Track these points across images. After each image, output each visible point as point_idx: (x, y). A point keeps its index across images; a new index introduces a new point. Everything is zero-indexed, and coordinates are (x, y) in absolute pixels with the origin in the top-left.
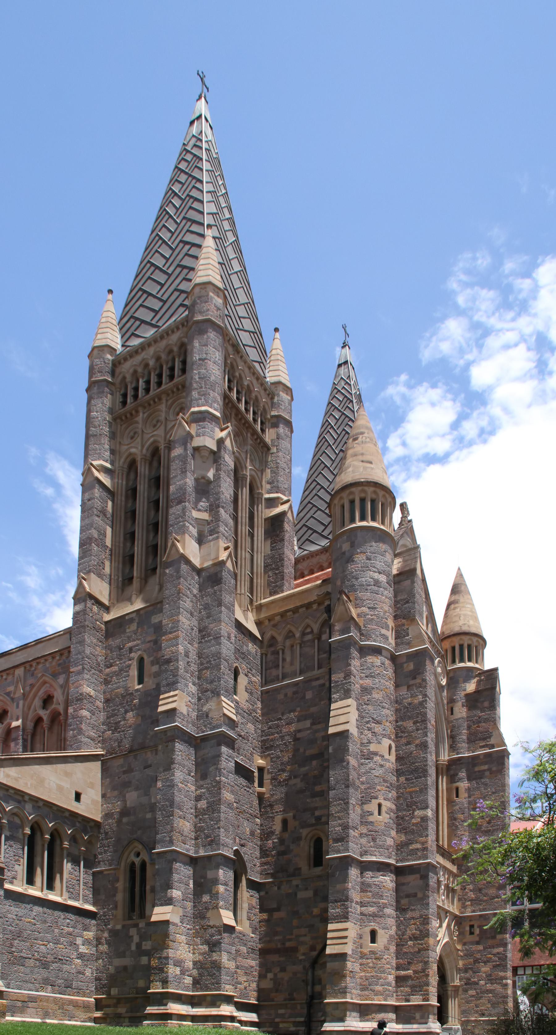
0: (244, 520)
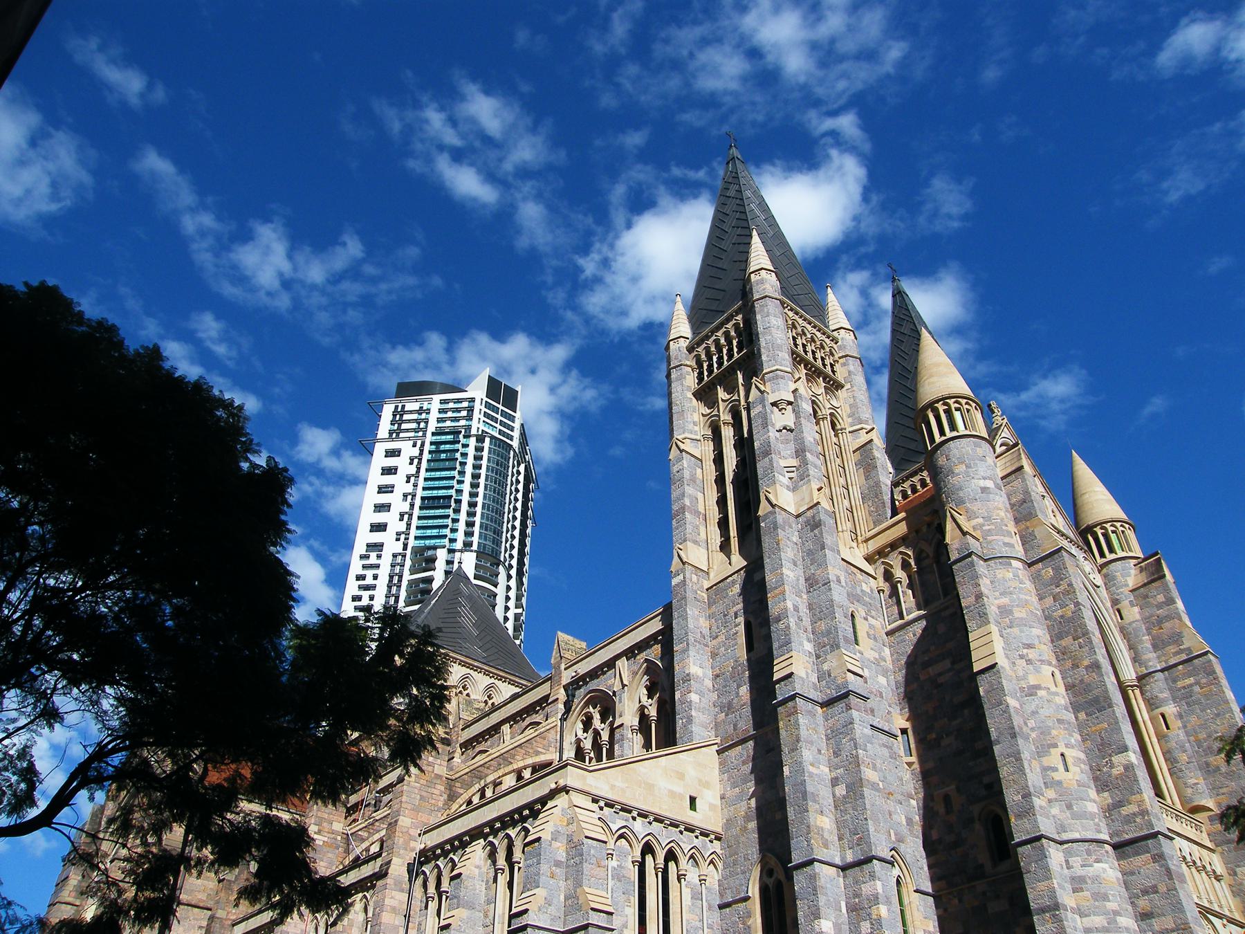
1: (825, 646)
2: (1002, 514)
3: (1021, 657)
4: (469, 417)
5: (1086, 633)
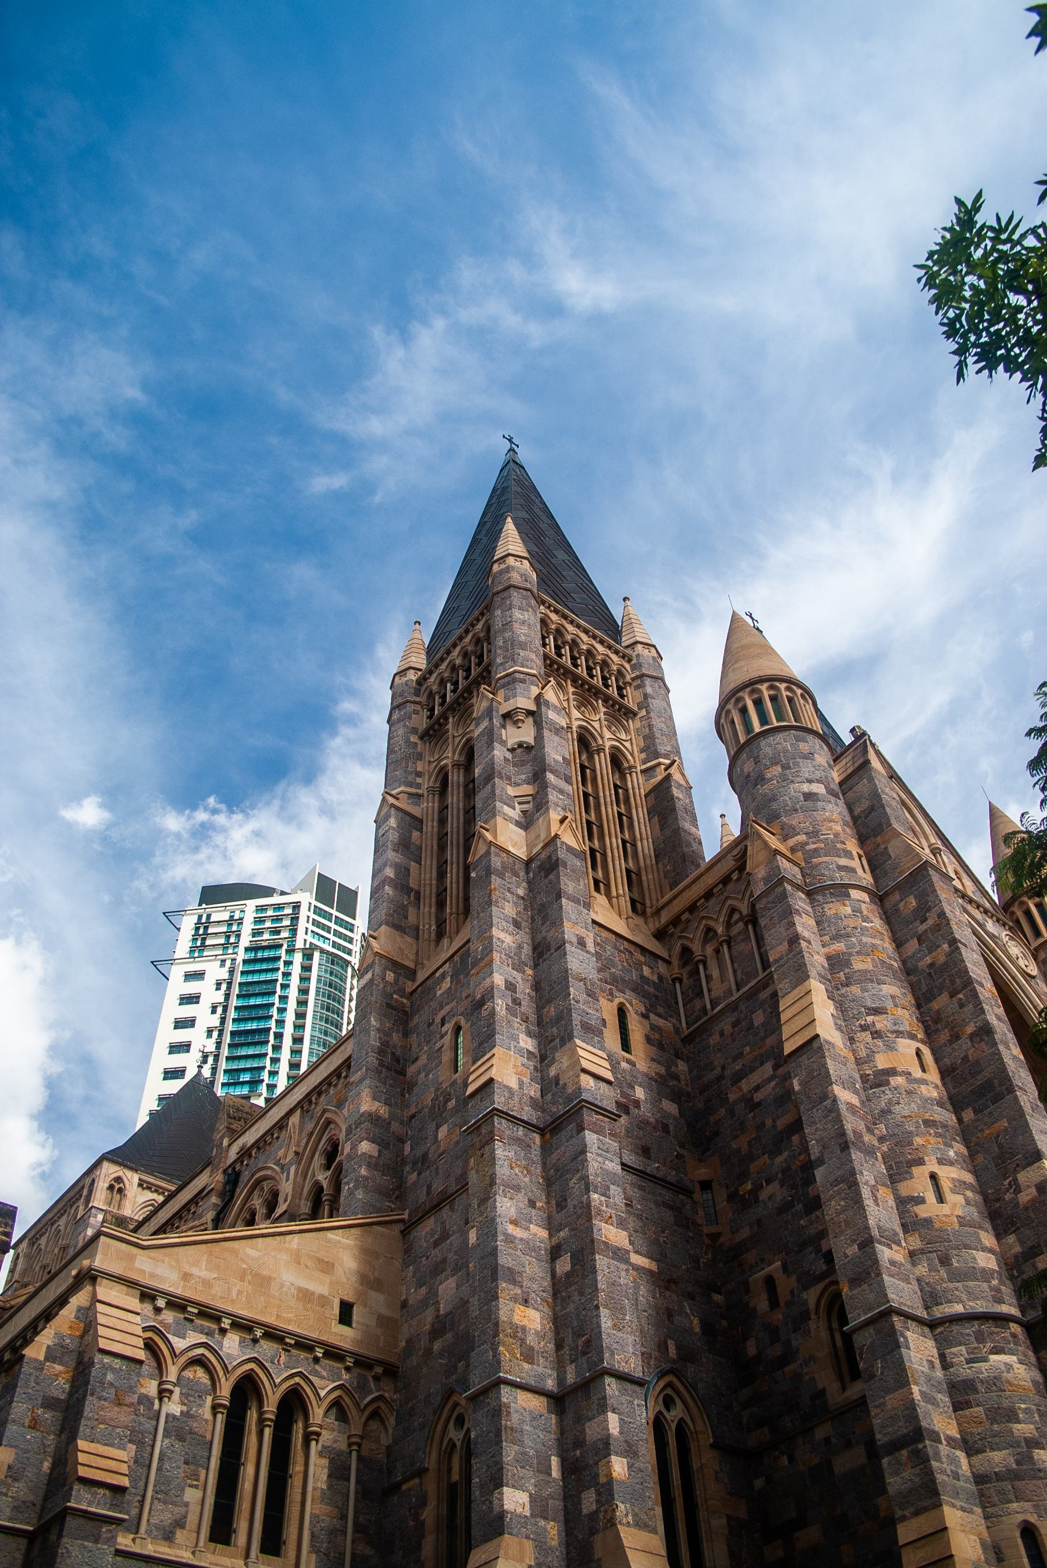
0: (608, 799)
1: (553, 1040)
2: (838, 828)
4: (294, 931)
5: (968, 983)
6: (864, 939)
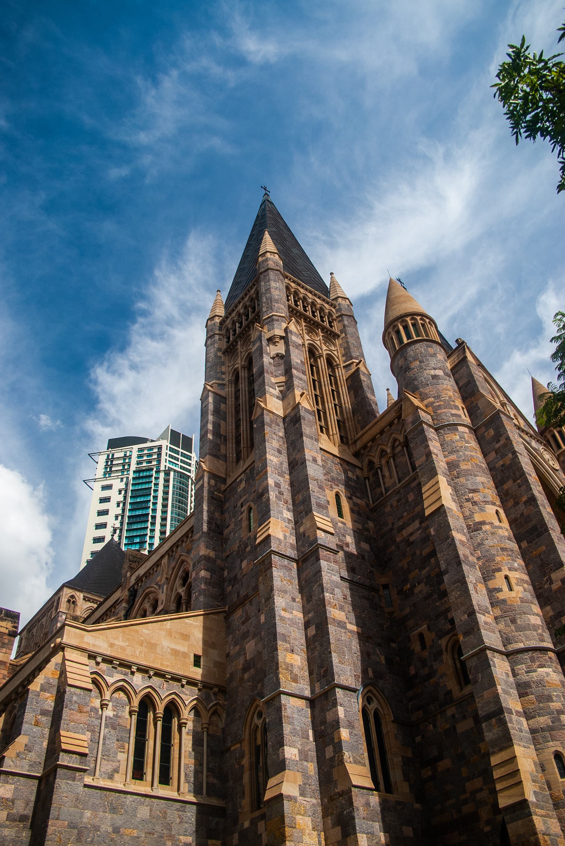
0: (326, 383)
1: (301, 513)
2: (451, 394)
3: (468, 500)
4: (159, 461)
5: (522, 474)
6: (466, 453)
